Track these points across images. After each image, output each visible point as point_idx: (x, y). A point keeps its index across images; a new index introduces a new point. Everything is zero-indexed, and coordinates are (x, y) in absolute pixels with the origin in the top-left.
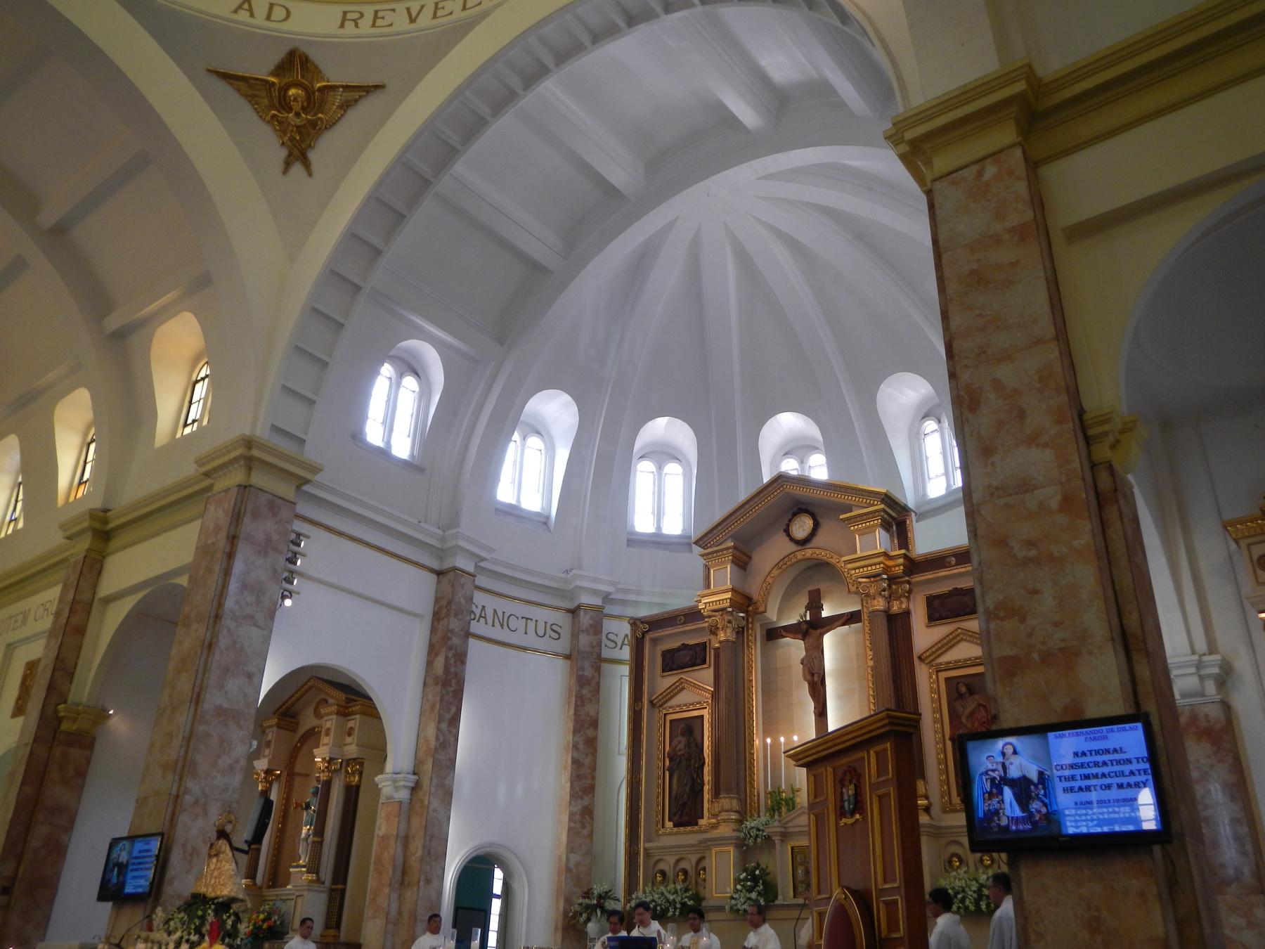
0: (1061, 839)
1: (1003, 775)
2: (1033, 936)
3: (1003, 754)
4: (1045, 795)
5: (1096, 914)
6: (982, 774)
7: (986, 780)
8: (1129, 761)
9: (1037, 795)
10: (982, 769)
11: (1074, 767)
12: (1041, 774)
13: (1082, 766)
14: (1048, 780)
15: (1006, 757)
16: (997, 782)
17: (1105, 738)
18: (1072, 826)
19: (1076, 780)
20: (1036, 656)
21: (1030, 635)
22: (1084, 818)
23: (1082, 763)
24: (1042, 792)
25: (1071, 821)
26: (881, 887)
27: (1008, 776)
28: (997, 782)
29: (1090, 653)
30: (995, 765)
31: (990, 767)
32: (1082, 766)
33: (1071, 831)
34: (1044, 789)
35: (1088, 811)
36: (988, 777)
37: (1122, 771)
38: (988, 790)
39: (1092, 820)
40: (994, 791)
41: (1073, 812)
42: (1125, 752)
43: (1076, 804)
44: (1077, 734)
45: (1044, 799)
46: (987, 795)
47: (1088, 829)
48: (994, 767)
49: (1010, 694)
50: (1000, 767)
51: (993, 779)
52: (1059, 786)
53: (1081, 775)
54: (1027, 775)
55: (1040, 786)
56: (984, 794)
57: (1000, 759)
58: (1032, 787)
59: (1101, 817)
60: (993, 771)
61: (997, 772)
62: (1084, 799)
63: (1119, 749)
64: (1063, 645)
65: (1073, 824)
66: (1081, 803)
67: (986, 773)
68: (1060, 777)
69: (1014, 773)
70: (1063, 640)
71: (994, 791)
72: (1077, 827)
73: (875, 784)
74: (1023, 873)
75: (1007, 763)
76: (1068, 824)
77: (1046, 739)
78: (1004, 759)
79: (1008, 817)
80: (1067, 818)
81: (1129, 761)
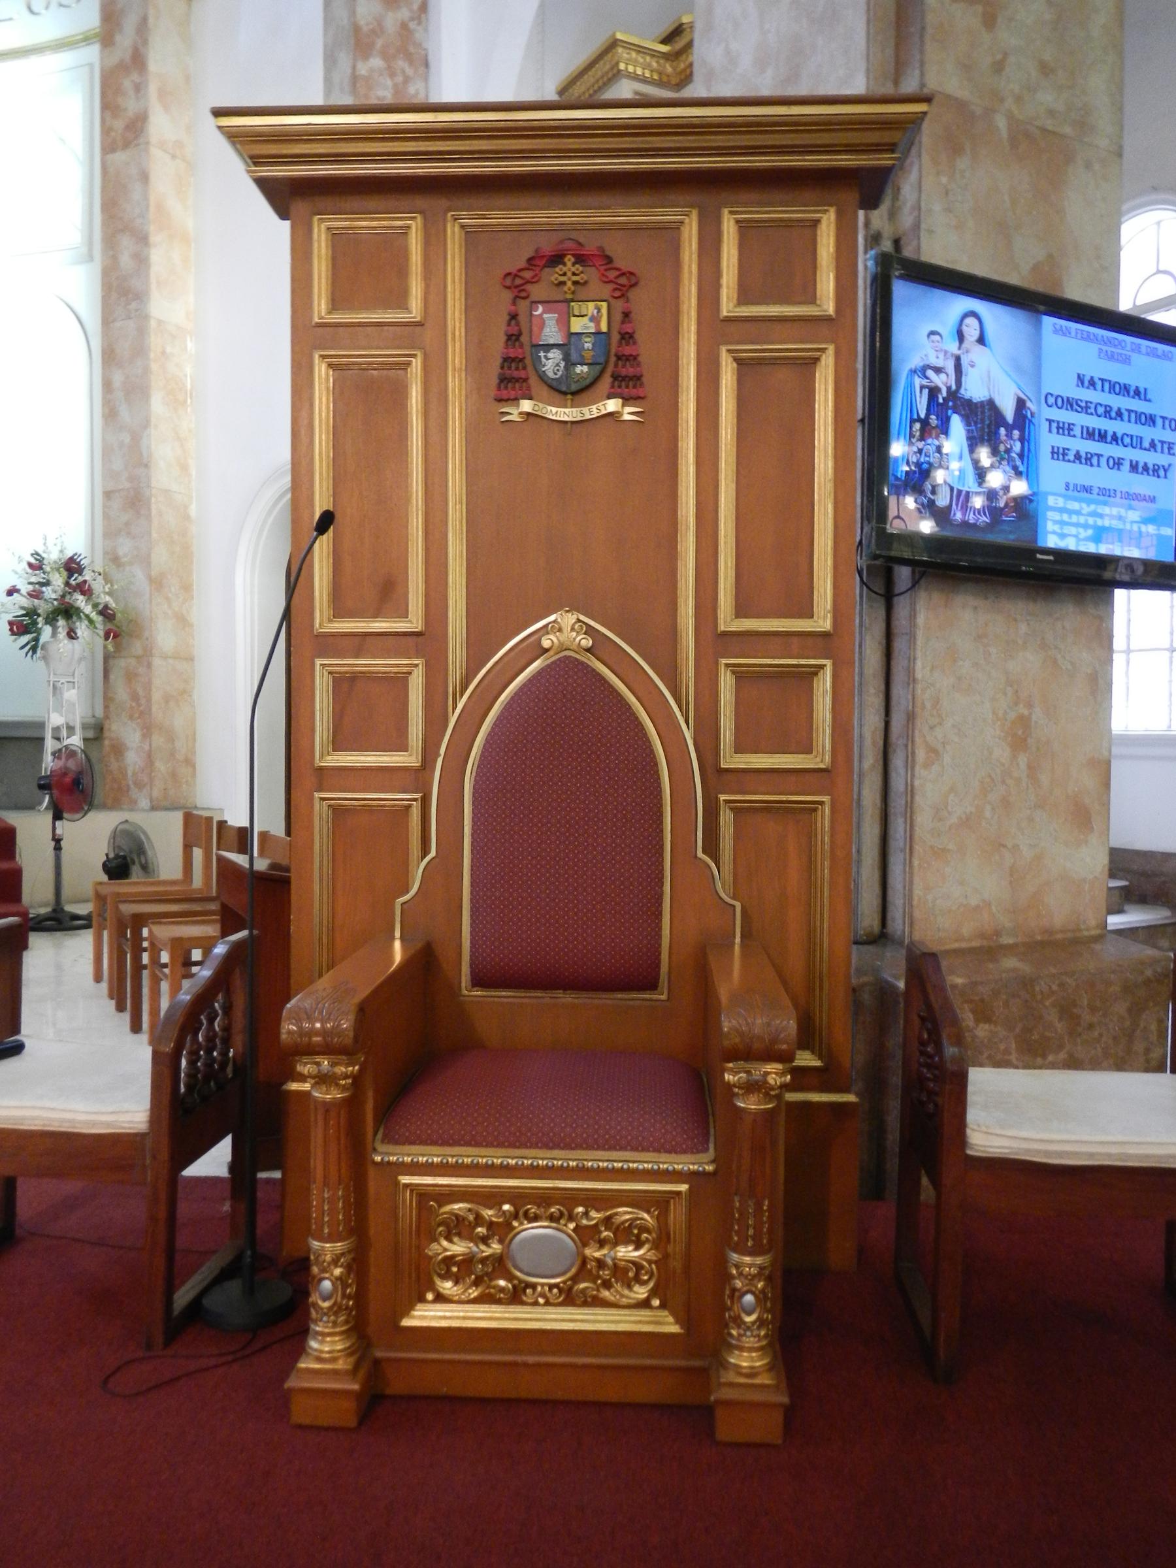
0: (1039, 556)
1: (954, 387)
2: (921, 755)
3: (961, 337)
4: (1021, 456)
5: (1026, 712)
6: (913, 372)
7: (922, 387)
8: (1151, 420)
9: (1008, 451)
10: (915, 362)
11: (1075, 406)
12: (1021, 404)
13: (1085, 408)
14: (1030, 421)
15: (964, 345)
16: (941, 400)
17: (1126, 361)
18: (1054, 533)
19: (1074, 436)
20: (1001, 123)
21: (998, 67)
22: (1074, 519)
23: (1087, 402)
24: (1017, 447)
25: (1055, 522)
26: (722, 627)
27: (962, 391)
28: (941, 400)
29: (1088, 166)
30: (941, 356)
31: (934, 361)
32: (1085, 408)
33: (1052, 542)
34: (1022, 440)
35: (1084, 505)
36: (925, 382)
37: (1141, 438)
38: (923, 416)
39: (1086, 526)
40: (934, 420)
41: (1060, 502)
42: (1149, 401)
43: (1067, 486)
44: (1088, 338)
45: (1018, 463)
46: (917, 426)
47: (1078, 545)
48: (939, 363)
49: (947, 194)
50: (950, 366)
51: (933, 392)
52: (1047, 440)
53: (1082, 427)
54: (998, 402)
55: (1016, 433)
56: (912, 421)
57: (953, 347)
58: (1002, 431)
59: (1100, 522)
60: (938, 370)
61: (943, 376)
62: (1082, 481)
63: (1142, 391)
64: (1049, 124)
65: (1056, 528)
66: (1076, 486)
67: (923, 371)
68: (1050, 421)
69: (974, 389)
70: (1051, 113)
71: (934, 420)
72: (1063, 536)
73: (728, 320)
74: (921, 620)
75: (965, 362)
76: (1050, 526)
77: (1038, 326)
78: (959, 348)
79: (952, 489)
80: (1050, 514)
81: (1151, 420)
